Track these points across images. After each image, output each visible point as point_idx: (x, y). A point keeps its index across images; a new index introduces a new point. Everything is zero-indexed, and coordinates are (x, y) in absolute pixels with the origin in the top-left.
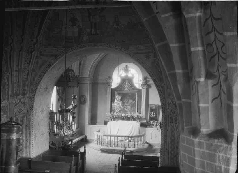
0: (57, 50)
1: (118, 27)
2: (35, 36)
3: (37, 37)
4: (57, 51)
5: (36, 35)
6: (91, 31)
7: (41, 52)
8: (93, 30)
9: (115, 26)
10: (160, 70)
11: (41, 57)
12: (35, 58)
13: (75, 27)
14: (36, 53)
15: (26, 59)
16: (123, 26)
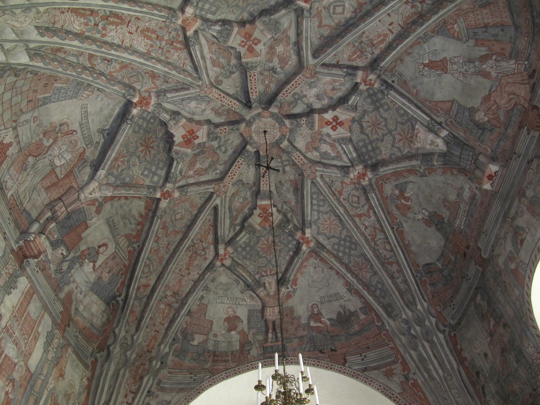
0: (195, 378)
1: (320, 325)
2: (157, 344)
3: (159, 345)
4: (194, 380)
5: (159, 340)
6: (266, 340)
7: (158, 384)
8: (270, 335)
9: (312, 324)
10: (423, 397)
11: (159, 393)
12: (146, 392)
13: (233, 333)
14: (151, 381)
15: (128, 391)
16: (328, 322)
